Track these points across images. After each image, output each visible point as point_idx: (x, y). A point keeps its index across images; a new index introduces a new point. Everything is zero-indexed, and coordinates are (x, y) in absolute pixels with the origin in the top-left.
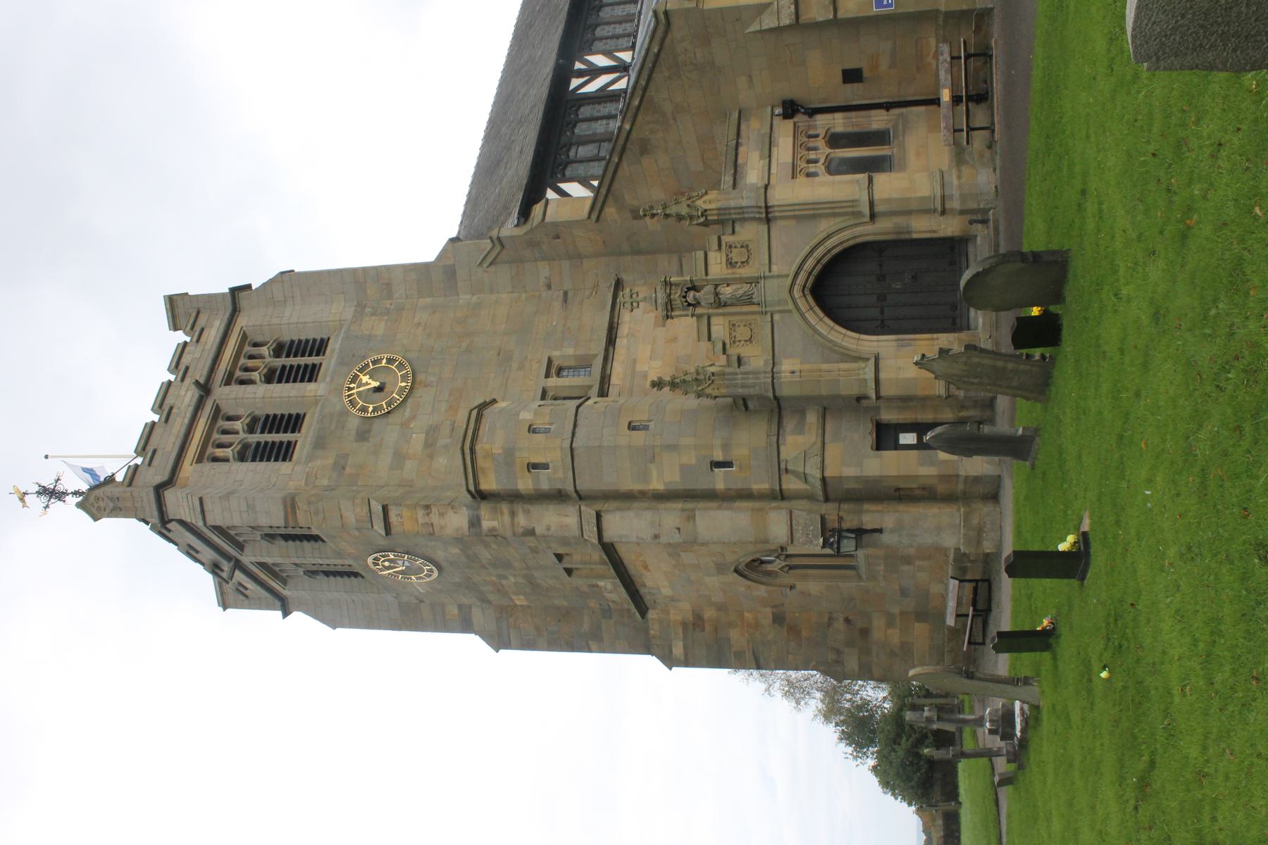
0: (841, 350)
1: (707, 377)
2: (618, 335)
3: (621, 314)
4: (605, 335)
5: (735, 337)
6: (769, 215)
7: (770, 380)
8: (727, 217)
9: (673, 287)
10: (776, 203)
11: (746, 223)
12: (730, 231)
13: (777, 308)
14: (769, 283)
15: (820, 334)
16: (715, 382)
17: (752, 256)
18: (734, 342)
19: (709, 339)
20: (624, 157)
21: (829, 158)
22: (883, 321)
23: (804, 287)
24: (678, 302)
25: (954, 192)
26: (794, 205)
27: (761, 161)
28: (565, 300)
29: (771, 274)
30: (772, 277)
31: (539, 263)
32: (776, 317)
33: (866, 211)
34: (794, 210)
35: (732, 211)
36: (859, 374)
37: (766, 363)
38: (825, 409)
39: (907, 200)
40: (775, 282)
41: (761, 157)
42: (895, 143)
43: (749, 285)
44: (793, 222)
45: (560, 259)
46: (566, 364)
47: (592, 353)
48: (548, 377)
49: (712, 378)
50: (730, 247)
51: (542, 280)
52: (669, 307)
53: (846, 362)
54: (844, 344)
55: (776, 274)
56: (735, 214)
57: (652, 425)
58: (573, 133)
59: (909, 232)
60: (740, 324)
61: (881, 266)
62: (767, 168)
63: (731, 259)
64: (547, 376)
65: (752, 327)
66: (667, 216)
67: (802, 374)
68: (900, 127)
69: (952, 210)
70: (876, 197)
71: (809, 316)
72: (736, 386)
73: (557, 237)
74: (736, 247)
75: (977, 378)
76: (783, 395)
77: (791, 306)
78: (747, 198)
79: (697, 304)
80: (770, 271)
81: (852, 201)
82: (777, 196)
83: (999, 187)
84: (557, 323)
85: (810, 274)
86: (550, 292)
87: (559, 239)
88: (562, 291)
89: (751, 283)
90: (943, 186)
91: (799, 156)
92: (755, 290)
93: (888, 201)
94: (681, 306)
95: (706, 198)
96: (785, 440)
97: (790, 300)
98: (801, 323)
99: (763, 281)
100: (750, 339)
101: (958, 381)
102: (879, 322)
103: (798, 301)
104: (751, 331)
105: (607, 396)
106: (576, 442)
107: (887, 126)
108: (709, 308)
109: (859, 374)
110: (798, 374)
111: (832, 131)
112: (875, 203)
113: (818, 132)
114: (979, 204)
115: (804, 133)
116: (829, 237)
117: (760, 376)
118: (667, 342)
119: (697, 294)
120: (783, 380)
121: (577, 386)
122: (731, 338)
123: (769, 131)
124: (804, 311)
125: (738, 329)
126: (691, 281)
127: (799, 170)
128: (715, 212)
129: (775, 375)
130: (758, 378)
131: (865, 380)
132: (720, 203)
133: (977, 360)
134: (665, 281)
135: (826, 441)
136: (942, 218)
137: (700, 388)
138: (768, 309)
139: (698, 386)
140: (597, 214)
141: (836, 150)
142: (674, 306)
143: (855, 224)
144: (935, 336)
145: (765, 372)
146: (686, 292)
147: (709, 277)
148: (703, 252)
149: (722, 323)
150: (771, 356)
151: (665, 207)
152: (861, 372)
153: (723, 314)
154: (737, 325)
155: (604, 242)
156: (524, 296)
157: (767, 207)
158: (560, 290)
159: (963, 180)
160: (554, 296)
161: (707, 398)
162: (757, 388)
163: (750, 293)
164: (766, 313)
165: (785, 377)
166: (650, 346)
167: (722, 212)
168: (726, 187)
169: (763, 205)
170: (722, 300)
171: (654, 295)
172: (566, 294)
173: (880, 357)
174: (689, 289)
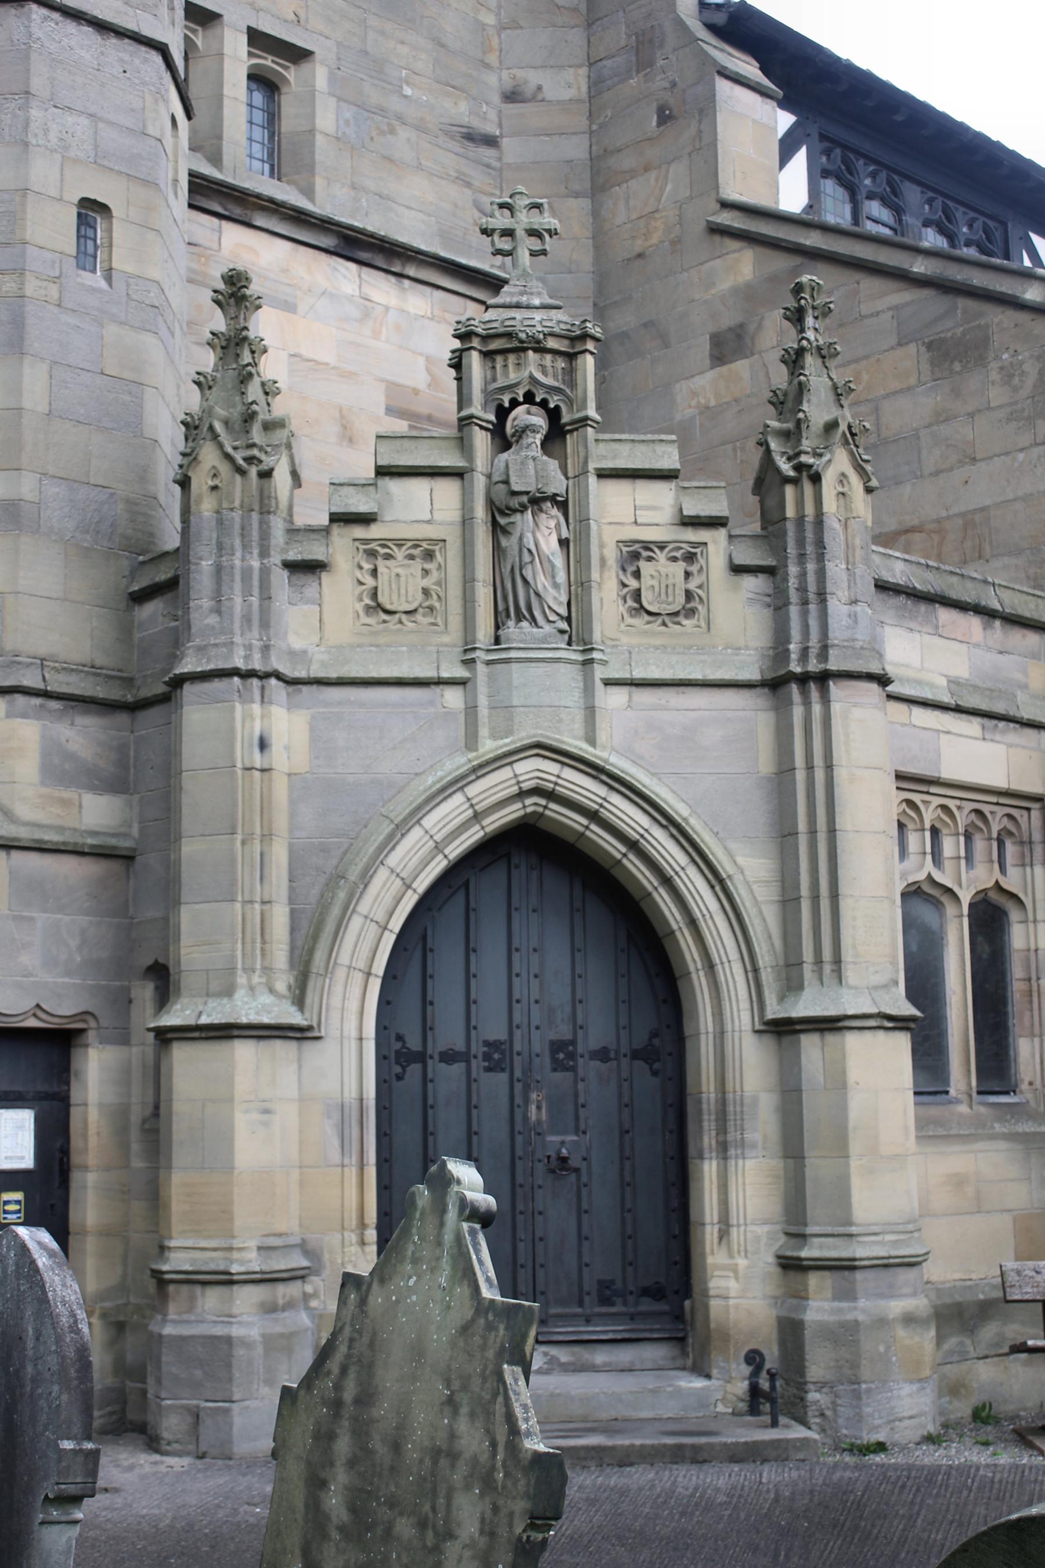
0: (336, 911)
1: (255, 452)
2: (365, 270)
3: (428, 290)
4: (370, 228)
5: (388, 557)
6: (794, 688)
7: (239, 662)
8: (792, 550)
9: (561, 363)
10: (836, 707)
11: (767, 613)
12: (740, 560)
13: (483, 701)
14: (569, 677)
15: (390, 842)
16: (238, 478)
17: (656, 626)
18: (372, 554)
19: (382, 472)
20: (926, 293)
21: (945, 899)
22: (421, 1057)
23: (550, 795)
24: (513, 376)
25: (862, 1303)
26: (829, 767)
27: (943, 682)
28: (473, 137)
29: (599, 685)
30: (588, 690)
31: (583, 71)
32: (453, 698)
33: (805, 1007)
34: (810, 768)
35: (811, 567)
36: (249, 970)
37: (300, 657)
38: (128, 858)
39: (841, 1146)
40: (572, 698)
41: (954, 683)
42: (982, 1109)
43: (563, 611)
44: (766, 765)
45: (591, 132)
46: (288, 105)
47: (319, 183)
48: (250, 43)
49: (253, 471)
50: (690, 558)
51: (533, 78)
52: (494, 345)
53: (293, 930)
54: (356, 923)
55: (598, 702)
56: (803, 575)
57: (97, 280)
58: (926, 224)
59: (723, 1149)
60: (435, 575)
61: (602, 1055)
62: (928, 694)
63: (650, 559)
64: (257, 38)
65: (419, 617)
66: (794, 360)
67: (257, 774)
68: (1027, 1127)
69: (801, 1296)
70: (853, 1041)
71: (454, 809)
72: (220, 547)
73: (665, 117)
74: (688, 575)
75: (353, 1509)
76: (186, 709)
77: (489, 746)
78: (854, 617)
79: (502, 440)
80: (608, 683)
81: (837, 961)
82: (857, 713)
83: (879, 1458)
84: (406, 97)
85: (593, 816)
86: (496, 99)
87: (659, 124)
88: (498, 133)
89: (568, 619)
90: (886, 1265)
91: (952, 804)
92: (548, 628)
93: (839, 1084)
94: (501, 382)
95: (856, 484)
96: (24, 715)
97: (508, 743)
98: (430, 780)
99: (579, 657)
100: (380, 607)
101: (337, 1405)
102: (414, 1043)
103: (506, 773)
104: (406, 612)
105: (191, 206)
106: (46, 18)
107: (1024, 1086)
108: (489, 476)
109: (249, 970)
110: (258, 760)
111: (1014, 915)
112: (831, 1038)
113: (1013, 872)
114: (821, 1386)
115: (1011, 827)
116: (717, 880)
117: (255, 633)
118: (342, 417)
119: (538, 438)
120: (238, 707)
121: (221, 120)
122: (384, 543)
123: (1026, 714)
124: (472, 790)
125: (417, 565)
126: (584, 421)
127: (916, 798)
128: (809, 510)
129: (255, 682)
130: (247, 619)
131: (228, 991)
132: (836, 525)
133: (469, 1527)
134: (585, 336)
135: (15, 855)
136: (771, 1259)
137: (218, 427)
138: (481, 669)
139: (226, 423)
140: (737, 224)
141: (966, 921)
142: (499, 360)
143: (756, 970)
144: (372, 1235)
145: (266, 649)
146: (544, 404)
147: (592, 480)
148: (678, 466)
149: (438, 516)
150: (321, 674)
151: (824, 354)
152: (256, 979)
153: (466, 522)
154: (427, 566)
155: (640, 256)
156: (490, 19)
157: (823, 678)
158: (500, 126)
159: (901, 1332)
160: (485, 108)
161: (184, 455)
162: (213, 620)
163: (537, 614)
164: (469, 663)
165: (248, 716)
166: (331, 360)
167: (810, 535)
168: (876, 559)
169: (833, 666)
170: (517, 518)
171: (537, 302)
172: (491, 141)
173: (308, 1045)
174: (553, 415)
